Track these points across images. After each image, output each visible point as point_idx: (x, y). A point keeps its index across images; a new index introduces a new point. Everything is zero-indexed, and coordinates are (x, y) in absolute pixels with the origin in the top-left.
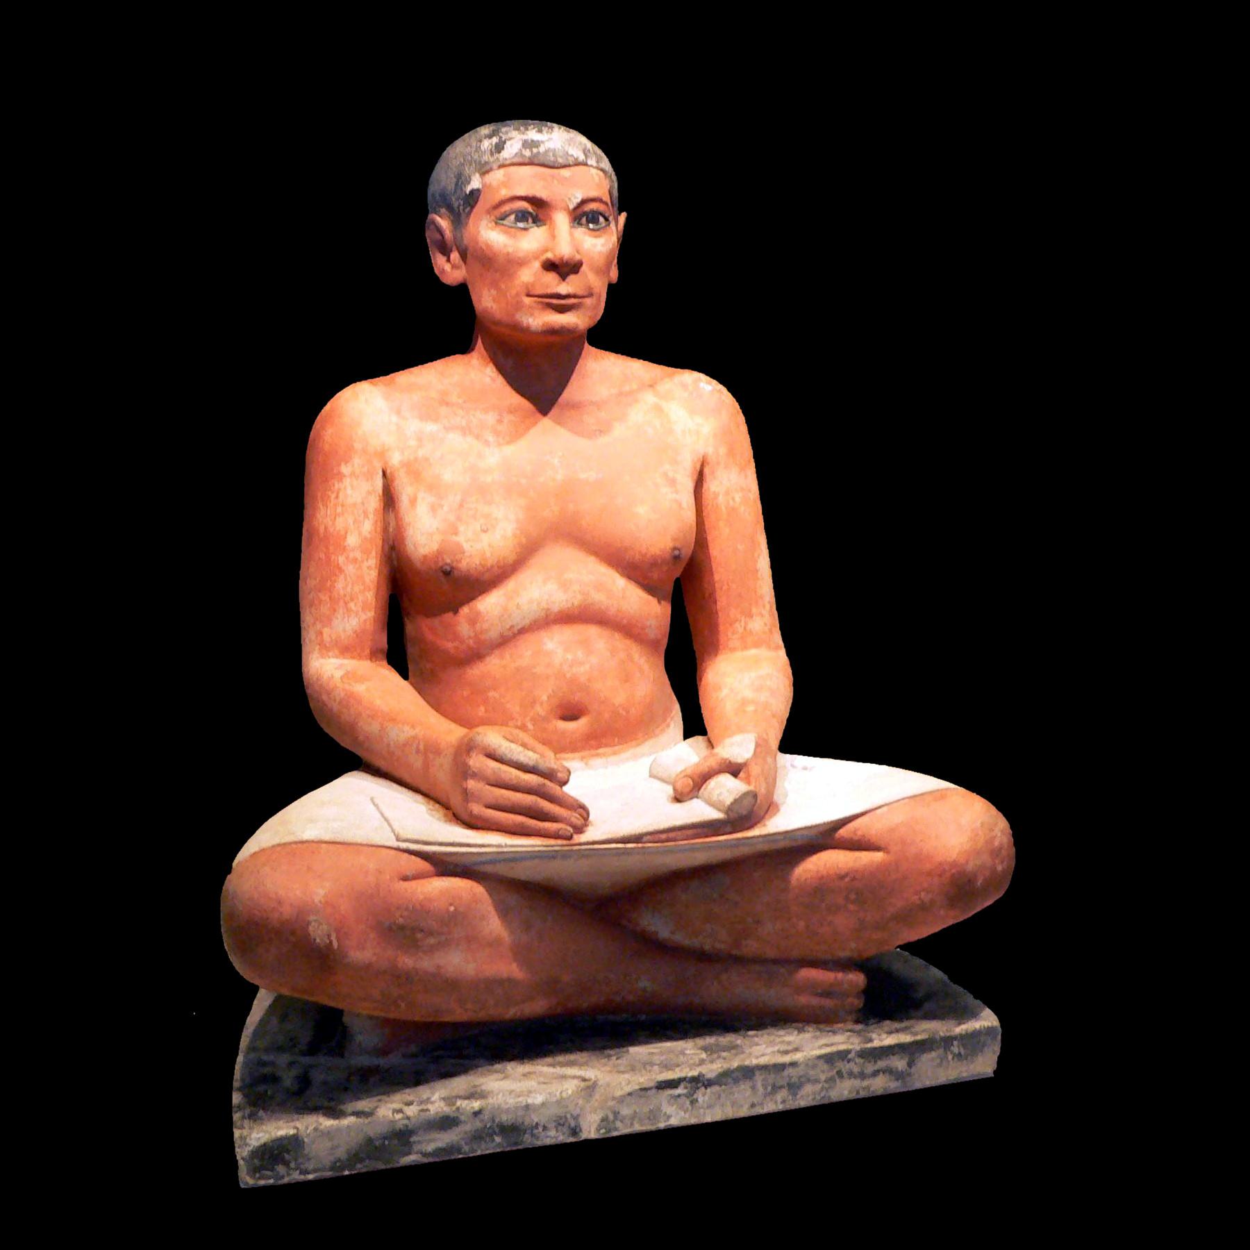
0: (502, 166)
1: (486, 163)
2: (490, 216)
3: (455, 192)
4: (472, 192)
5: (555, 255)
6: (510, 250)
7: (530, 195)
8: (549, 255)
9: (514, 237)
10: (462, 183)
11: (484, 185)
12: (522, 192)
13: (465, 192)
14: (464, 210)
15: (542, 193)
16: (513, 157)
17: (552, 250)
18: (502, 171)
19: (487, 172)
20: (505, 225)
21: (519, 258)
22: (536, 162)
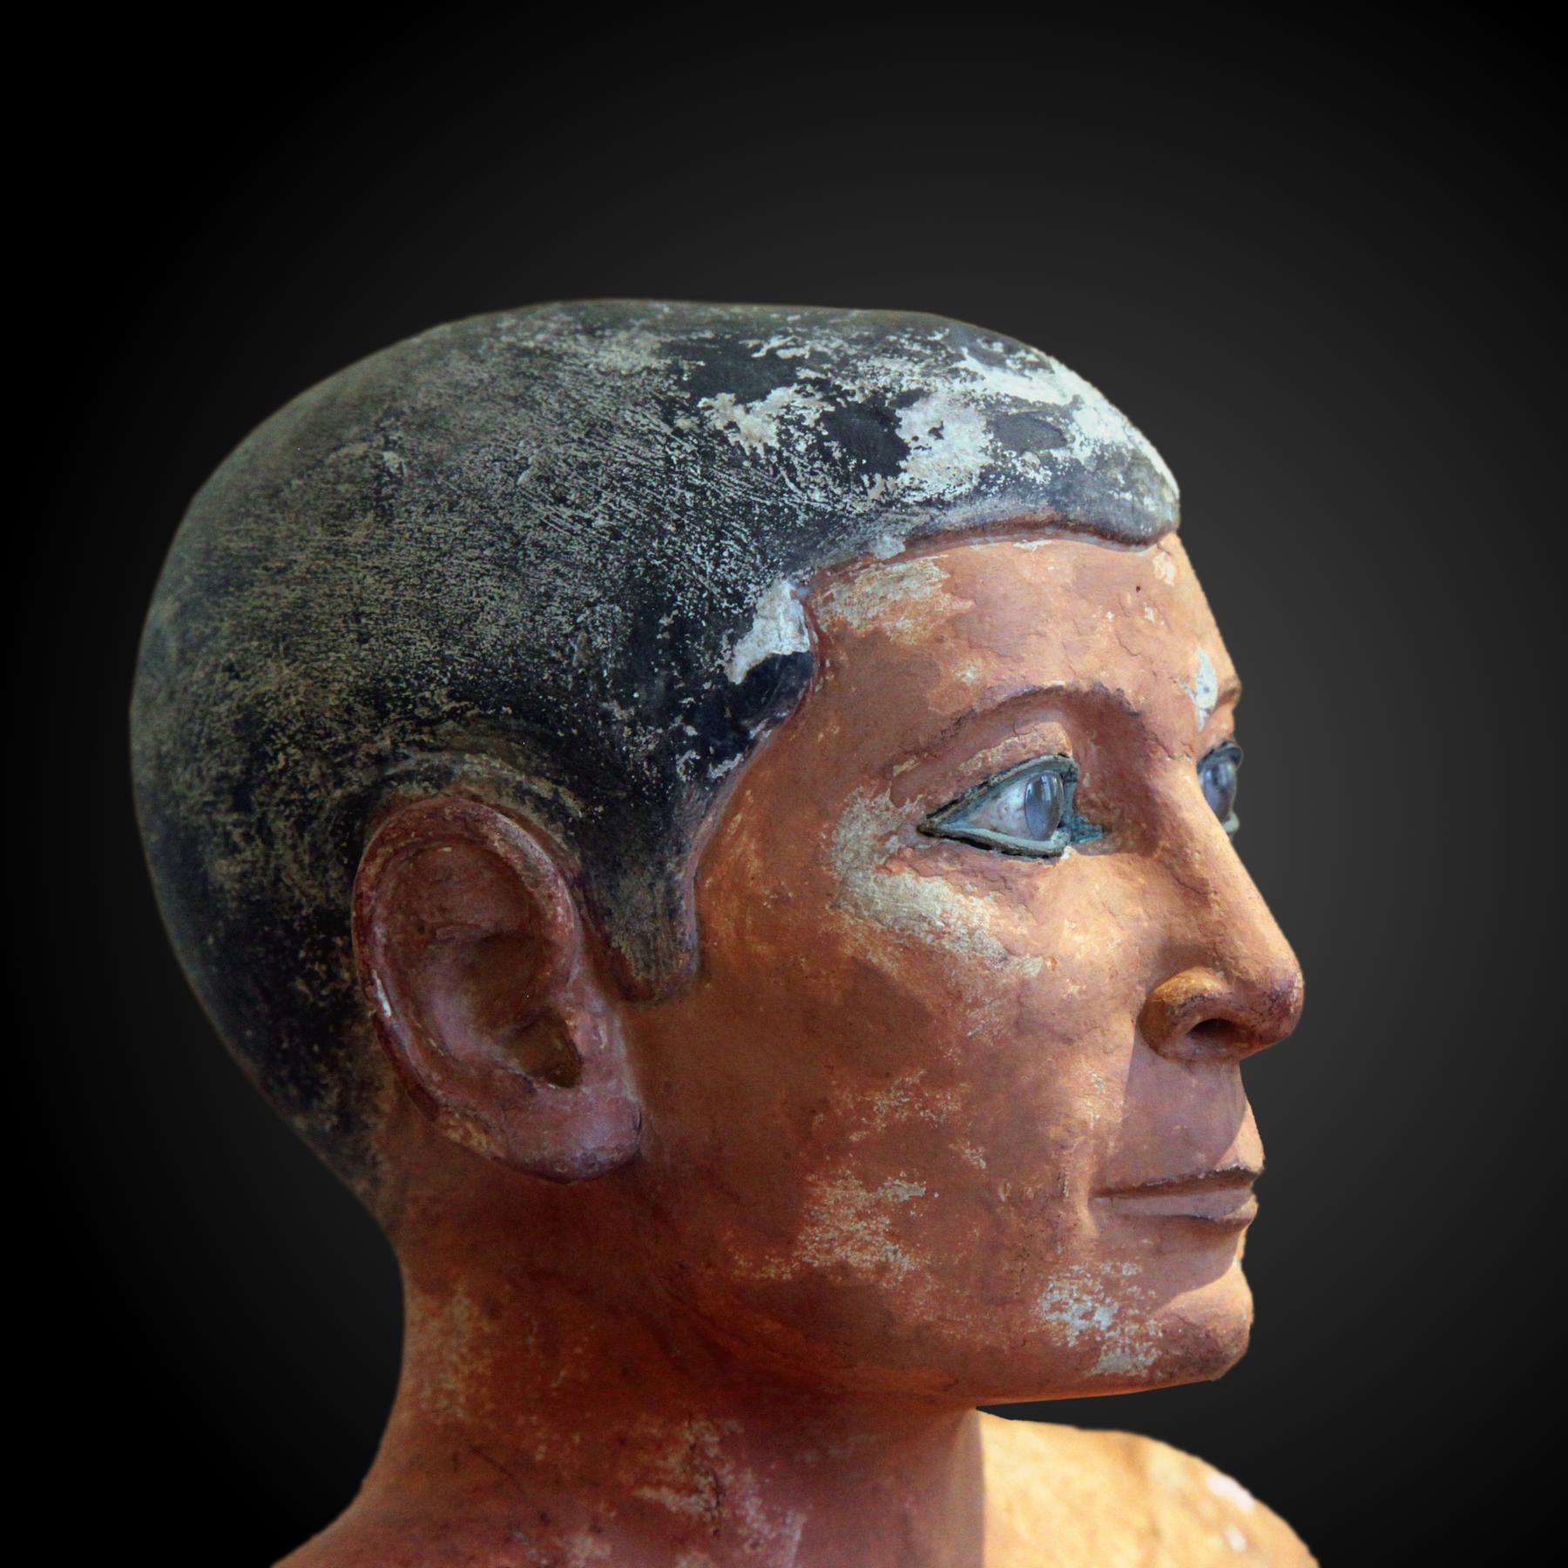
0: (921, 540)
1: (828, 524)
2: (898, 801)
3: (626, 680)
4: (769, 674)
5: (1244, 985)
6: (1032, 968)
7: (1085, 687)
8: (1207, 983)
9: (1025, 900)
10: (681, 626)
11: (824, 643)
12: (1054, 676)
13: (720, 677)
14: (699, 769)
15: (1122, 678)
16: (977, 492)
17: (1209, 955)
18: (929, 569)
19: (842, 572)
20: (984, 845)
21: (1068, 1005)
22: (1076, 512)
